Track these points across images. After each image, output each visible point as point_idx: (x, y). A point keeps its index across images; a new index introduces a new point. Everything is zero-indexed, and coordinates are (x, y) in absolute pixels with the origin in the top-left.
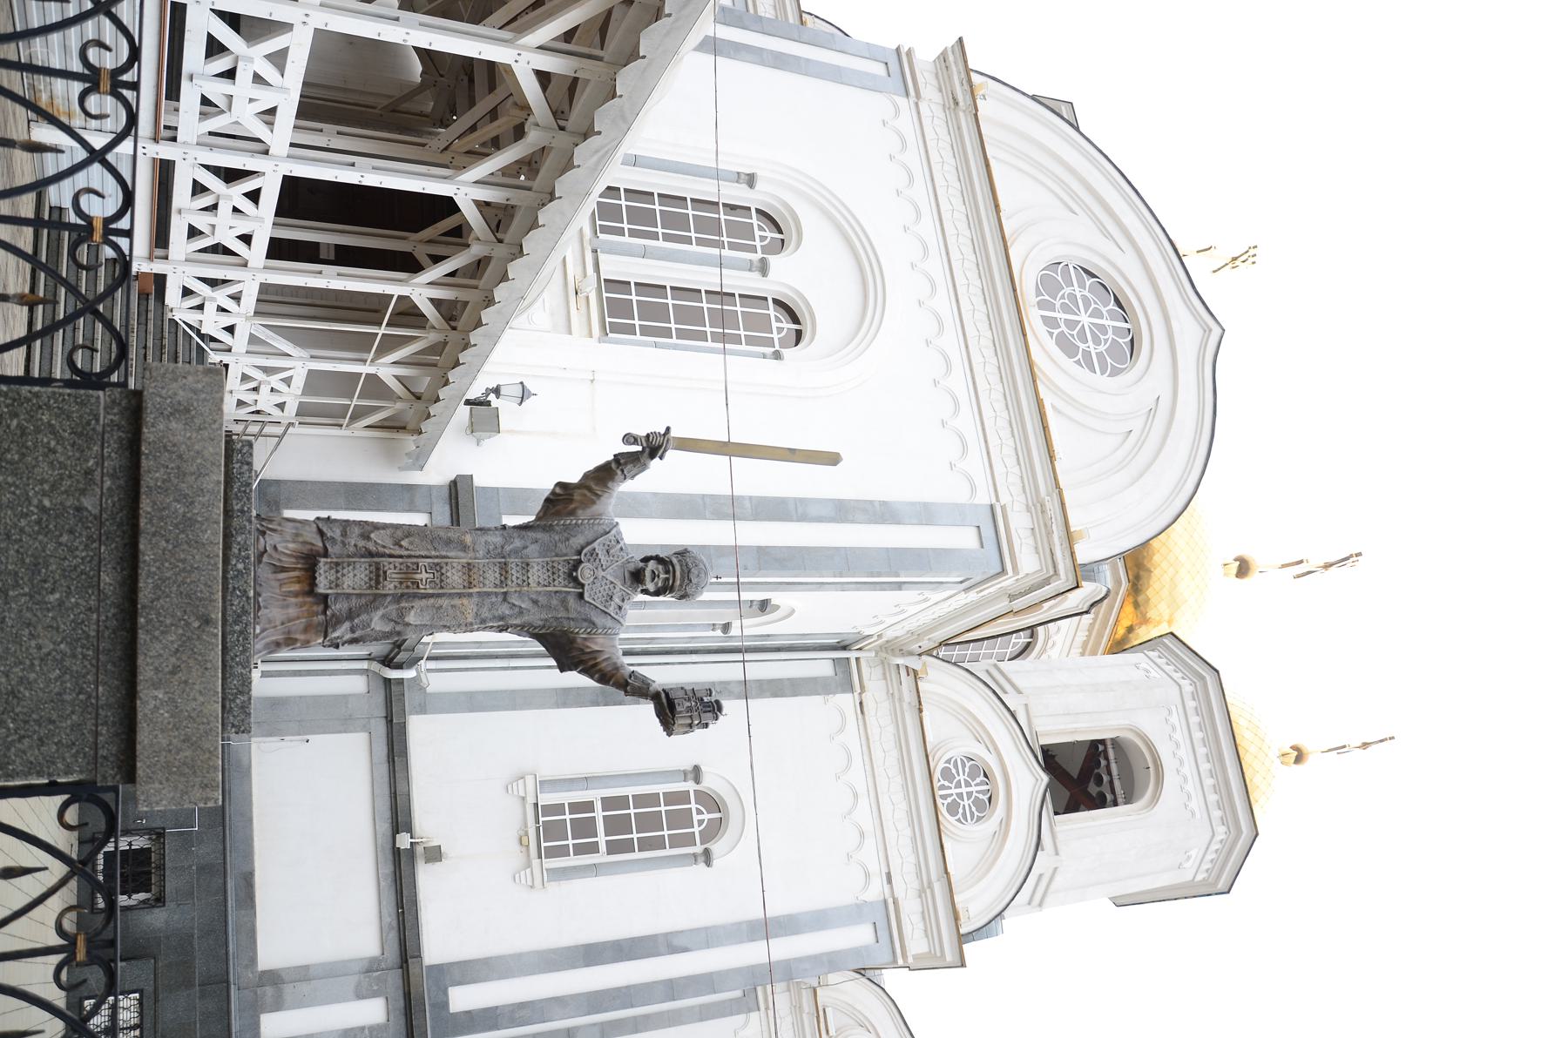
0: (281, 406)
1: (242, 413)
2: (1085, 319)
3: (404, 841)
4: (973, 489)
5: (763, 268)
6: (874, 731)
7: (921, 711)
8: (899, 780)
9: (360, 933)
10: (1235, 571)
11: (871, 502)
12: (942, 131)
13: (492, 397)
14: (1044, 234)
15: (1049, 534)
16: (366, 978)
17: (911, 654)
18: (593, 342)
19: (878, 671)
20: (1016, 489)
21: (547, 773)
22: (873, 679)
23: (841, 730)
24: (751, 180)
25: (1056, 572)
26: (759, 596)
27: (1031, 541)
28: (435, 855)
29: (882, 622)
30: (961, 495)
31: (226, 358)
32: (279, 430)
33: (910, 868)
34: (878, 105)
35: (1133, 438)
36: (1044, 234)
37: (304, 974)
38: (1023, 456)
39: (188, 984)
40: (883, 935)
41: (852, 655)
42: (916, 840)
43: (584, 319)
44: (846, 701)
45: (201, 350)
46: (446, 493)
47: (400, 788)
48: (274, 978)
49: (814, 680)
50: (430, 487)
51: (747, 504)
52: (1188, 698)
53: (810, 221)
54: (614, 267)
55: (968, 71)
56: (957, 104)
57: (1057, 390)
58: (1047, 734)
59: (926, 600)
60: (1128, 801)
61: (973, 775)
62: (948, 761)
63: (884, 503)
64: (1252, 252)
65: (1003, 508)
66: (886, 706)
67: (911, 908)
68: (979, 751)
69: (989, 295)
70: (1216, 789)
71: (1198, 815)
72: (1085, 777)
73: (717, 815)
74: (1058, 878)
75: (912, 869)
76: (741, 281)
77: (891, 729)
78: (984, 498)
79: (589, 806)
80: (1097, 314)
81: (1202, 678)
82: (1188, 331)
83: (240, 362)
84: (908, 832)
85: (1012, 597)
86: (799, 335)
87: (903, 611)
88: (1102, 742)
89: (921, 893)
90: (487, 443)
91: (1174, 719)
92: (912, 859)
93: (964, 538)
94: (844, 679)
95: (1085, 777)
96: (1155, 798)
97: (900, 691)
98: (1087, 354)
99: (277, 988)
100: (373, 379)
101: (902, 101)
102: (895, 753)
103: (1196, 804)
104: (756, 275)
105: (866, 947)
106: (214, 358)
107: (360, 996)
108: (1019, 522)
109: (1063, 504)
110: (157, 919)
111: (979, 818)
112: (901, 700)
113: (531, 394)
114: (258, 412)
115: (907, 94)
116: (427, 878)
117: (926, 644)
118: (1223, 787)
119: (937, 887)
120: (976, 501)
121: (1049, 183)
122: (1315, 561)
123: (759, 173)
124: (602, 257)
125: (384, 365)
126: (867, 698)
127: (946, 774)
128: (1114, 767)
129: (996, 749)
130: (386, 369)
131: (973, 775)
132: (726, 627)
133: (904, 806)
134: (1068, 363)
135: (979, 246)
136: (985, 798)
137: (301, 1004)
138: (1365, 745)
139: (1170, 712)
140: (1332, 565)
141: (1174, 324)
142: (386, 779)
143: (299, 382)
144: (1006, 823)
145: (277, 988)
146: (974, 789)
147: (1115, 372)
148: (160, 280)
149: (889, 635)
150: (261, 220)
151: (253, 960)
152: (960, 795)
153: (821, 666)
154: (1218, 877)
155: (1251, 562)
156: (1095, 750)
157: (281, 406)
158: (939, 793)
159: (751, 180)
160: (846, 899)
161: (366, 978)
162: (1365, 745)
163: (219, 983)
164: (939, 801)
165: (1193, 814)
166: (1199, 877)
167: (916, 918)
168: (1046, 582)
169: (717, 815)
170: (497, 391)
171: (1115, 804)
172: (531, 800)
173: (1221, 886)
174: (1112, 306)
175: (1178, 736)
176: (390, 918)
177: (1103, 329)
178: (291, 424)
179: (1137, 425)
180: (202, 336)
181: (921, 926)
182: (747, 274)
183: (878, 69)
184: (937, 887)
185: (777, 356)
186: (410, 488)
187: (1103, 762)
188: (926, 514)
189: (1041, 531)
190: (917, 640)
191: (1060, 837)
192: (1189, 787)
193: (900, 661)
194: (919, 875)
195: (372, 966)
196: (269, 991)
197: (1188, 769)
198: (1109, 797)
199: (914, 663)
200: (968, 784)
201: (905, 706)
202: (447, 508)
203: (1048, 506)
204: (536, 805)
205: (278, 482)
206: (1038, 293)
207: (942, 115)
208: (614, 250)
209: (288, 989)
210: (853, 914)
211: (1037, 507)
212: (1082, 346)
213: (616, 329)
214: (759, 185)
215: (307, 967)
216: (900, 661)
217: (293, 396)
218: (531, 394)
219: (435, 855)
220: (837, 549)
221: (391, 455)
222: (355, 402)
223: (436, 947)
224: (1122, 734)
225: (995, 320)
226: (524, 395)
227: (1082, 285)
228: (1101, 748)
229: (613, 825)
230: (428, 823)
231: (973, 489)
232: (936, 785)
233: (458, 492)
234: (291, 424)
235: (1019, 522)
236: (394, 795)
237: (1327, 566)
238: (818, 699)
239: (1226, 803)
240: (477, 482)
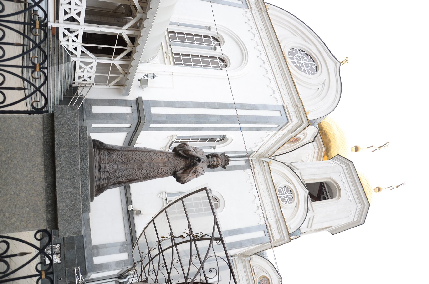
0: (90, 78)
1: (80, 81)
2: (302, 62)
3: (130, 208)
4: (277, 101)
5: (215, 49)
6: (258, 179)
7: (271, 173)
8: (267, 192)
9: (119, 235)
10: (354, 150)
11: (250, 104)
12: (259, 17)
13: (146, 78)
14: (289, 41)
15: (300, 112)
16: (122, 248)
17: (266, 157)
18: (172, 66)
19: (258, 163)
20: (289, 102)
21: (169, 191)
22: (257, 168)
23: (249, 179)
24: (209, 28)
25: (303, 122)
26: (222, 133)
27: (295, 115)
28: (139, 212)
29: (257, 146)
30: (275, 103)
31: (75, 59)
32: (90, 86)
33: (272, 215)
34: (241, 11)
35: (319, 90)
36: (289, 41)
37: (105, 246)
38: (290, 93)
39: (73, 248)
40: (266, 233)
41: (250, 159)
42: (273, 208)
43: (169, 61)
44: (249, 171)
45: (69, 56)
46: (135, 101)
47: (128, 196)
49: (240, 166)
50: (131, 100)
51: (216, 104)
52: (345, 170)
53: (226, 38)
54: (176, 49)
55: (264, 3)
56: (262, 10)
57: (297, 78)
58: (307, 180)
59: (268, 135)
60: (332, 197)
61: (287, 191)
62: (280, 188)
63: (254, 105)
64: (347, 59)
65: (286, 106)
66: (261, 172)
67: (274, 226)
68: (288, 184)
69: (276, 55)
70: (356, 194)
71: (352, 201)
72: (320, 192)
73: (217, 203)
74: (315, 220)
75: (273, 216)
76: (210, 53)
77: (263, 178)
78: (281, 103)
80: (306, 60)
81: (348, 164)
82: (331, 64)
83: (78, 59)
84: (271, 206)
85: (292, 133)
86: (226, 66)
87: (262, 141)
88: (322, 183)
89: (276, 222)
90: (145, 89)
91: (342, 175)
92: (273, 213)
93: (277, 114)
94: (249, 165)
95: (320, 192)
96: (339, 197)
97: (264, 168)
98: (304, 70)
99: (98, 250)
100: (113, 64)
101: (247, 10)
102: (265, 185)
103: (351, 198)
104: (213, 51)
105: (262, 237)
106: (72, 59)
107: (121, 252)
108: (291, 110)
109: (302, 104)
111: (290, 203)
112: (265, 170)
113: (156, 76)
114: (84, 80)
115: (248, 8)
117: (270, 153)
118: (358, 193)
119: (281, 220)
120: (279, 104)
121: (288, 29)
122: (377, 147)
123: (211, 26)
124: (172, 47)
125: (116, 60)
126: (255, 170)
127: (280, 191)
128: (327, 189)
129: (293, 184)
130: (116, 61)
131: (287, 191)
132: (214, 148)
133: (269, 199)
134: (300, 72)
135: (272, 43)
136: (292, 197)
138: (397, 187)
139: (340, 174)
140: (381, 147)
141: (327, 62)
142: (124, 194)
143: (94, 68)
144: (298, 204)
145: (98, 250)
146: (288, 195)
147: (312, 74)
148: (57, 29)
149: (260, 152)
150: (82, 6)
151: (91, 243)
152: (284, 197)
153: (242, 163)
154: (360, 219)
155: (359, 148)
156: (321, 185)
157: (90, 78)
158: (279, 196)
159: (209, 28)
160: (255, 224)
161: (122, 248)
162: (397, 187)
163: (82, 248)
164: (279, 198)
165: (351, 201)
166: (355, 220)
167: (276, 229)
168: (301, 125)
169: (217, 203)
170: (147, 75)
171: (328, 199)
172: (165, 198)
173: (361, 222)
174: (309, 58)
175: (344, 180)
176: (128, 231)
177: (308, 64)
178: (93, 84)
179: (320, 87)
180: (69, 51)
181: (277, 231)
182: (211, 50)
183: (241, 3)
184: (281, 220)
185: (221, 69)
186: (126, 101)
187: (323, 188)
188: (265, 107)
189: (297, 112)
190: (267, 153)
191: (314, 208)
192: (349, 193)
193: (263, 159)
194: (275, 217)
195: (123, 244)
196: (95, 251)
197: (348, 189)
198: (326, 197)
199: (268, 160)
200: (286, 194)
201: (266, 172)
202: (136, 105)
203: (298, 105)
204: (166, 200)
205: (91, 99)
206: (289, 55)
207: (258, 13)
208: (174, 45)
209: (100, 250)
210: (257, 228)
211: (296, 106)
212: (303, 68)
213: (177, 64)
214: (212, 30)
215: (105, 244)
216: (263, 159)
217: (93, 74)
218: (156, 76)
219: (139, 212)
220: (242, 116)
221: (119, 92)
222: (110, 75)
224: (328, 180)
225: (278, 61)
226: (154, 76)
227: (301, 54)
228: (322, 184)
231: (277, 101)
232: (278, 194)
233: (138, 101)
234: (93, 84)
235: (291, 110)
236: (127, 198)
237: (380, 147)
238: (242, 171)
239: (360, 198)
240: (143, 99)
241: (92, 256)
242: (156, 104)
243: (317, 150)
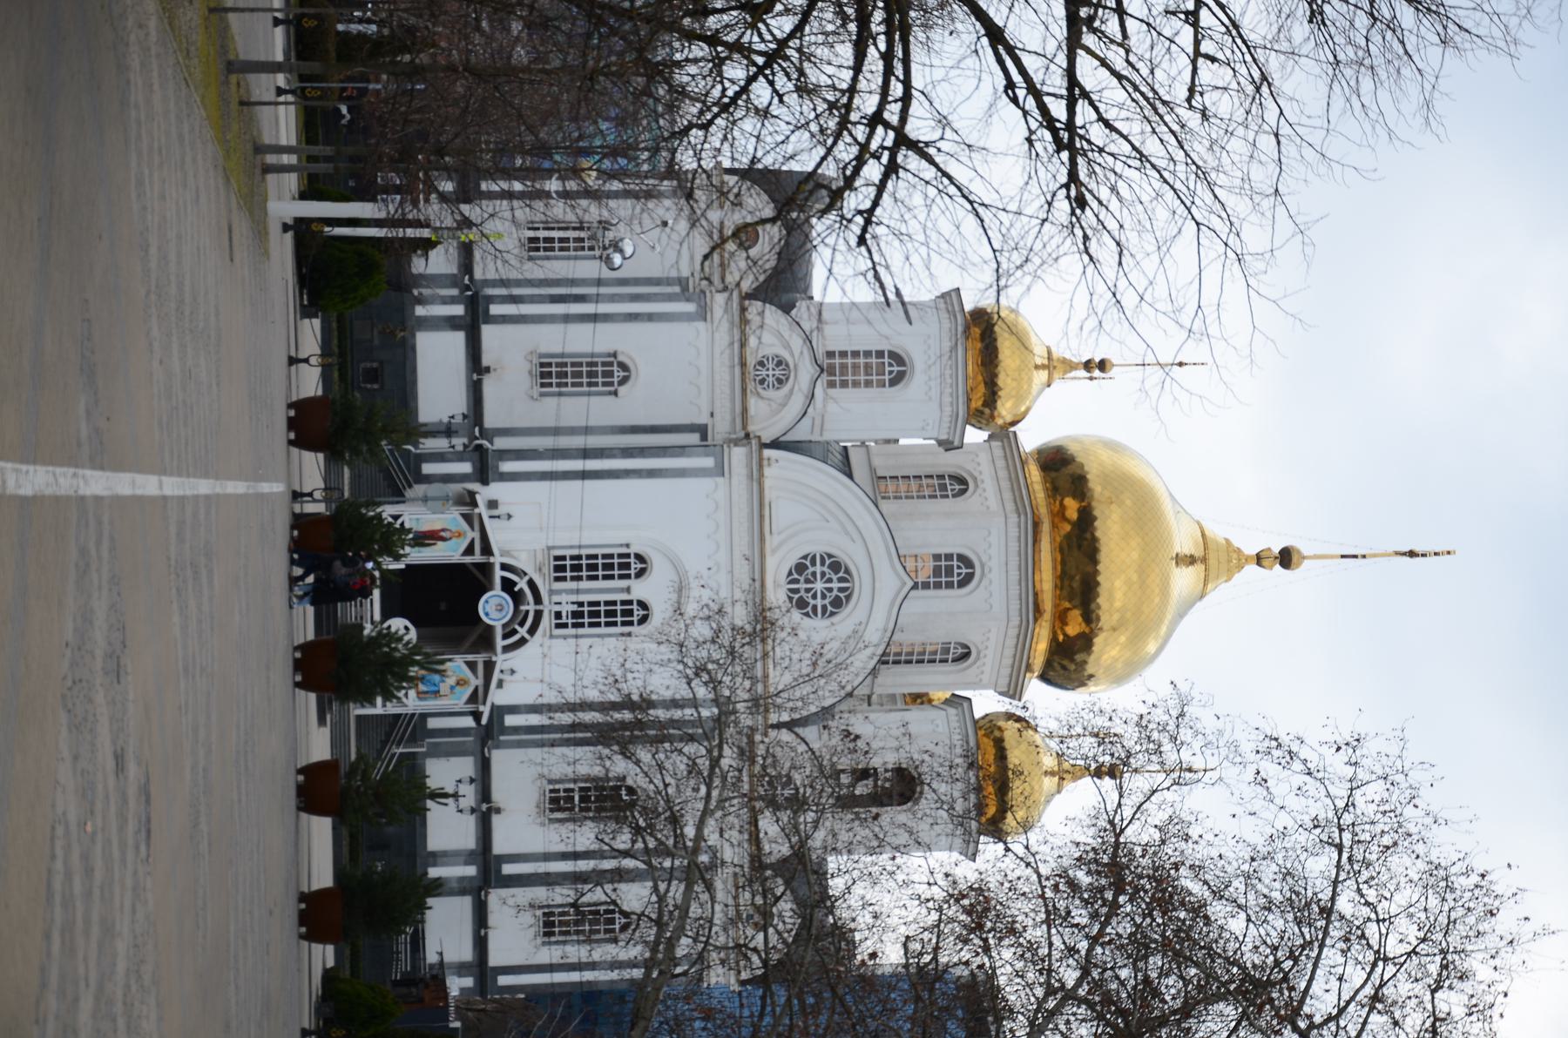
5: (628, 590)
16: (468, 857)
28: (498, 811)
34: (706, 483)
37: (445, 854)
48: (434, 854)
79: (572, 790)
101: (720, 480)
107: (467, 863)
110: (390, 830)
116: (495, 819)
137: (443, 865)
145: (436, 858)
159: (628, 546)
161: (468, 857)
185: (629, 634)
195: (471, 853)
219: (498, 811)
223: (499, 846)
229: (582, 799)
230: (497, 795)
241: (428, 865)
242: (514, 709)
243: (1015, 621)
